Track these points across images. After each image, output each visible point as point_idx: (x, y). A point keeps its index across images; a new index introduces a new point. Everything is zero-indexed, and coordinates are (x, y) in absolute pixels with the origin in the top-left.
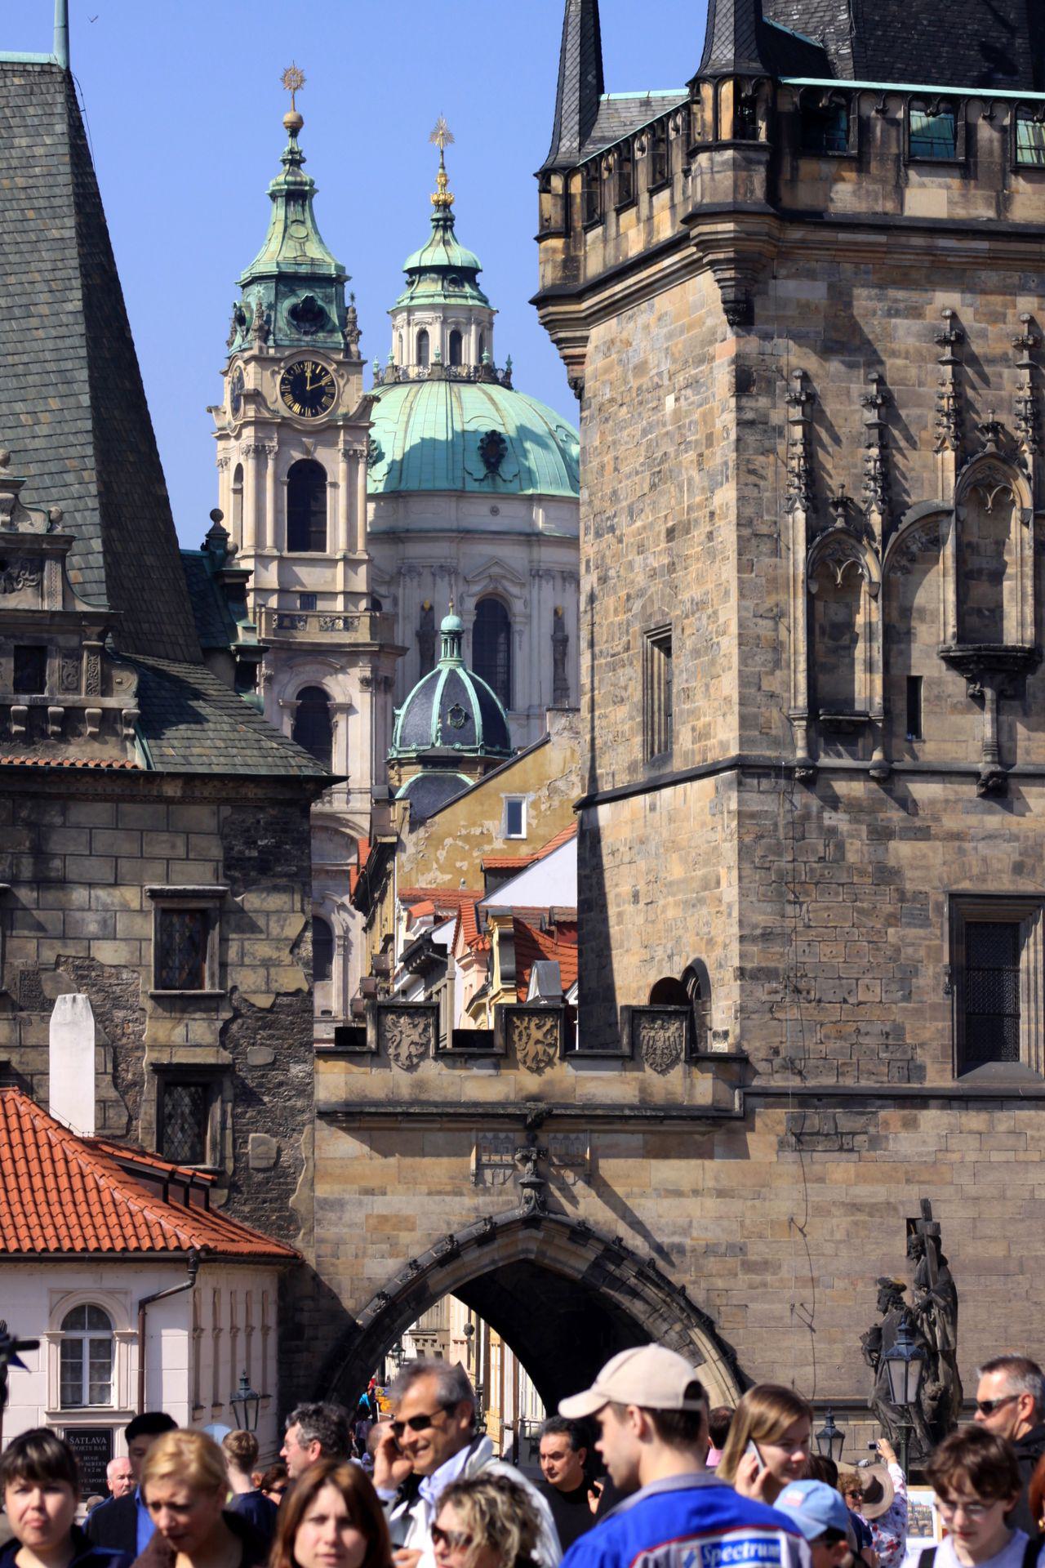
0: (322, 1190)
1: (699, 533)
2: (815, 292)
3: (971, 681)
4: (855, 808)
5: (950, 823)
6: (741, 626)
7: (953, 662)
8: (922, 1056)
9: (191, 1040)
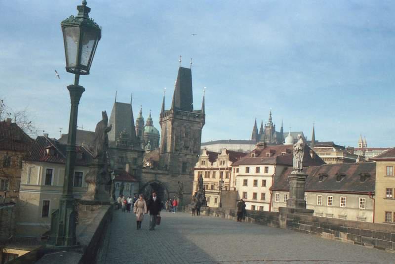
9: (135, 167)
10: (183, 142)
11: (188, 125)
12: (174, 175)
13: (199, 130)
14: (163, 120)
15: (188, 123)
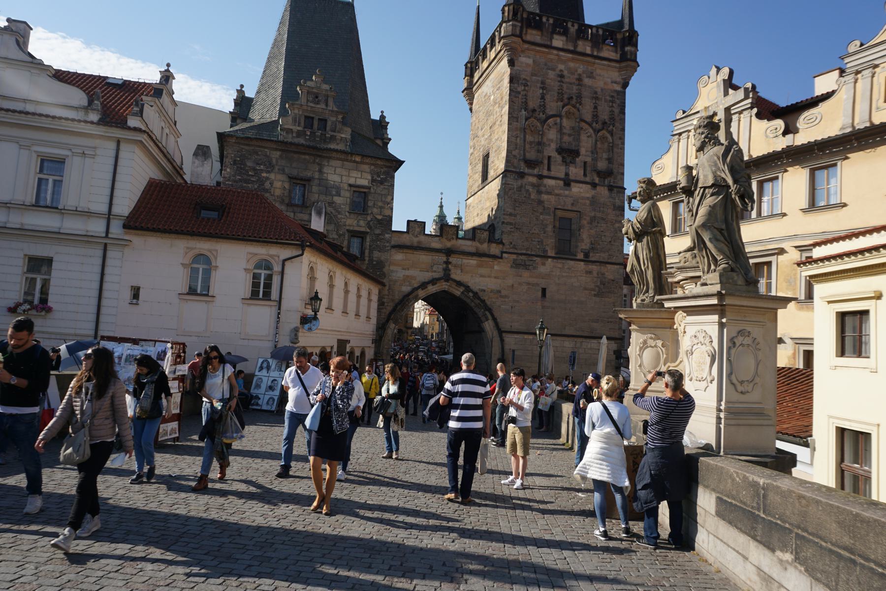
0: (392, 268)
1: (498, 123)
2: (530, 61)
3: (563, 158)
4: (533, 185)
5: (556, 191)
6: (508, 138)
7: (559, 153)
8: (547, 248)
10: (552, 134)
11: (572, 72)
12: (524, 261)
13: (618, 92)
14: (475, 81)
15: (572, 65)
